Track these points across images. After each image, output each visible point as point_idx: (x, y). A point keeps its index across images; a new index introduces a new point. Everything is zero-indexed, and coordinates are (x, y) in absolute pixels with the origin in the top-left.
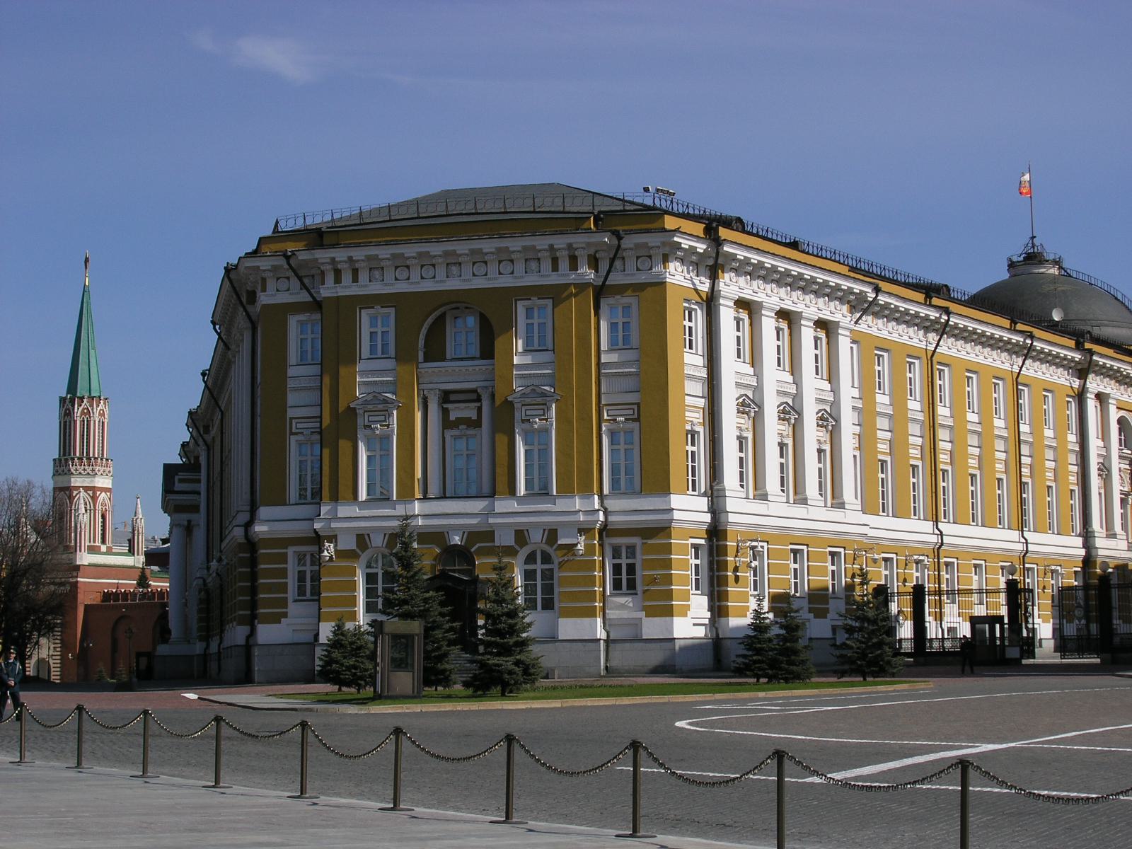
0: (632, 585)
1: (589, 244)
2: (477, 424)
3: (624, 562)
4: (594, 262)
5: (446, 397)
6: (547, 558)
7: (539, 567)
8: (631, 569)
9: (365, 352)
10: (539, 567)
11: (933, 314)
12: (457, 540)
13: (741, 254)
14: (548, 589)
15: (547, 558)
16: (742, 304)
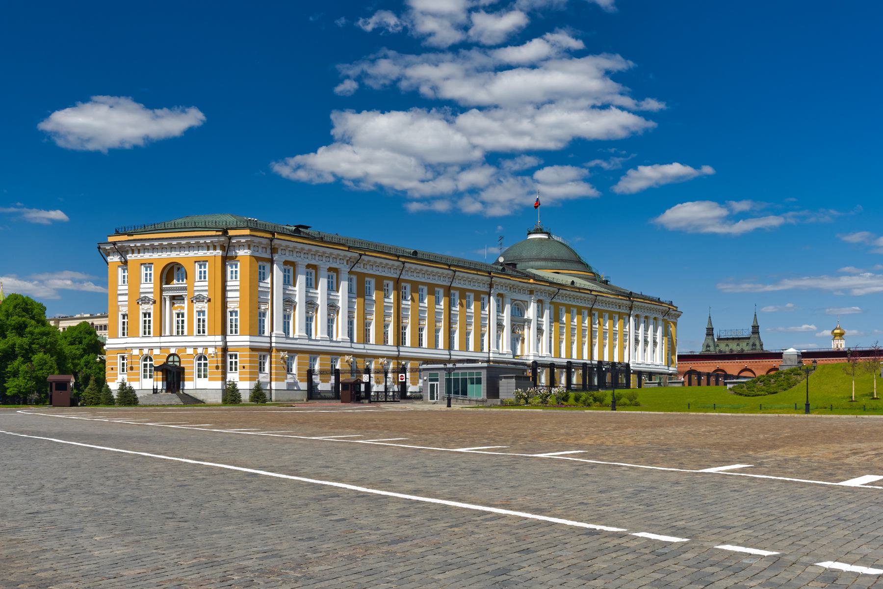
0: (236, 369)
1: (219, 241)
2: (183, 308)
3: (234, 360)
4: (223, 248)
5: (173, 298)
6: (205, 359)
7: (203, 362)
8: (236, 362)
9: (143, 280)
10: (203, 362)
11: (397, 263)
12: (172, 351)
13: (284, 243)
14: (205, 370)
15: (205, 359)
16: (286, 263)
